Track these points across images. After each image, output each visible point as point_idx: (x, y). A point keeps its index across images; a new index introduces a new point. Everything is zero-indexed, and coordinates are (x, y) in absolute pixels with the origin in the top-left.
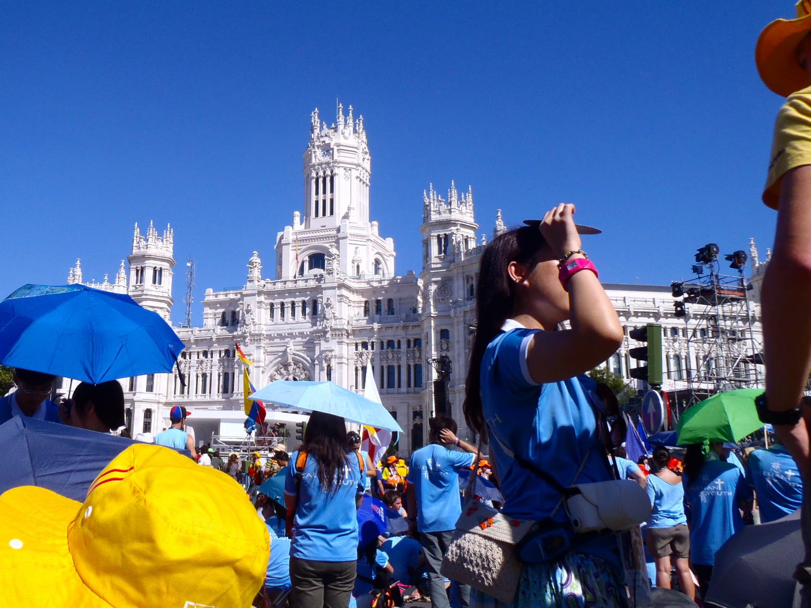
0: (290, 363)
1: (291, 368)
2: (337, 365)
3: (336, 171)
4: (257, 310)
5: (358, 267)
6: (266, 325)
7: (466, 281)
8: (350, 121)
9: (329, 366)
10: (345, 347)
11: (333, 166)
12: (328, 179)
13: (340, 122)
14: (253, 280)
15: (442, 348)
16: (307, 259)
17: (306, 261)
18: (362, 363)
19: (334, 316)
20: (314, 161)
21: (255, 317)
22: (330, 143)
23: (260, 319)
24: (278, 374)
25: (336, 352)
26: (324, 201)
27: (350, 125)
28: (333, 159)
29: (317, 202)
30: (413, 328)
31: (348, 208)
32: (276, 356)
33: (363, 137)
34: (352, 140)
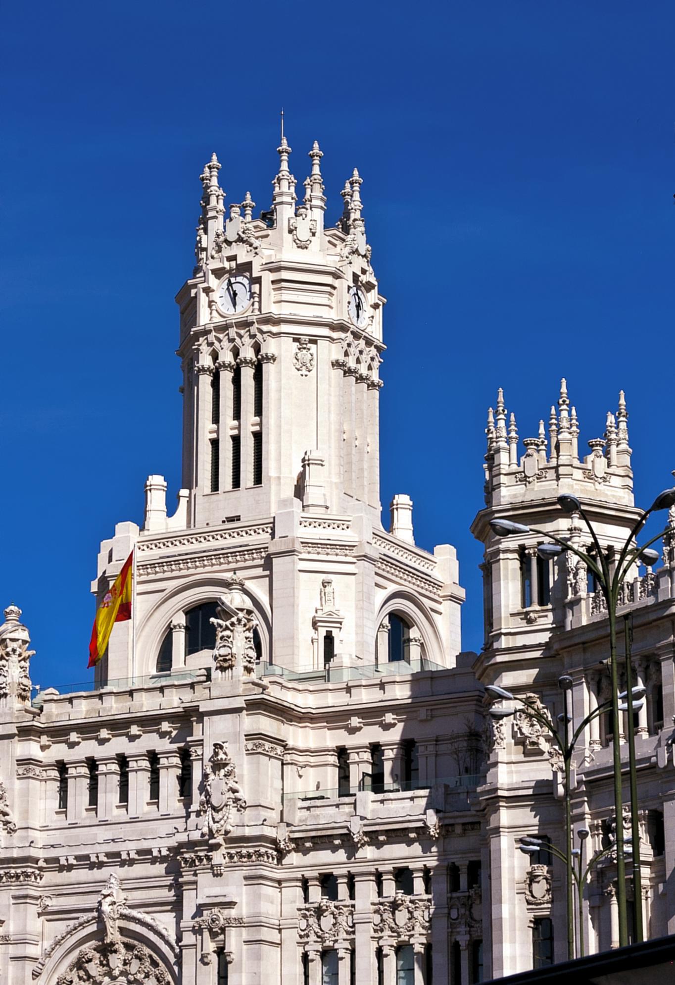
0: (112, 944)
1: (116, 961)
2: (245, 947)
3: (270, 347)
4: (18, 784)
5: (329, 640)
6: (45, 829)
8: (316, 193)
9: (220, 952)
11: (262, 332)
12: (247, 374)
13: (281, 194)
16: (181, 619)
18: (321, 938)
19: (237, 800)
21: (13, 806)
22: (251, 263)
23: (25, 813)
27: (315, 202)
30: (465, 830)
31: (303, 460)
32: (72, 923)
33: (358, 238)
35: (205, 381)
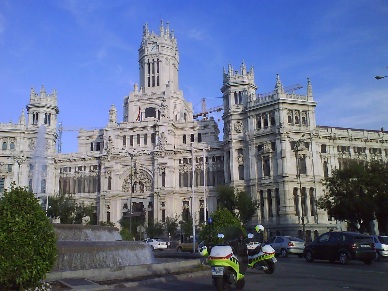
1: (138, 176)
5: (176, 115)
7: (255, 119)
10: (173, 161)
12: (156, 64)
13: (162, 30)
14: (113, 122)
15: (239, 160)
16: (144, 111)
17: (144, 112)
19: (166, 143)
20: (146, 54)
22: (157, 42)
24: (129, 179)
25: (169, 165)
26: (153, 77)
28: (159, 52)
29: (149, 78)
31: (169, 82)
34: (168, 42)
35: (146, 66)
